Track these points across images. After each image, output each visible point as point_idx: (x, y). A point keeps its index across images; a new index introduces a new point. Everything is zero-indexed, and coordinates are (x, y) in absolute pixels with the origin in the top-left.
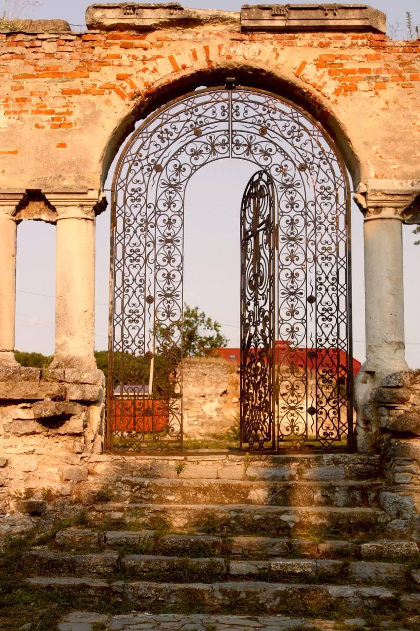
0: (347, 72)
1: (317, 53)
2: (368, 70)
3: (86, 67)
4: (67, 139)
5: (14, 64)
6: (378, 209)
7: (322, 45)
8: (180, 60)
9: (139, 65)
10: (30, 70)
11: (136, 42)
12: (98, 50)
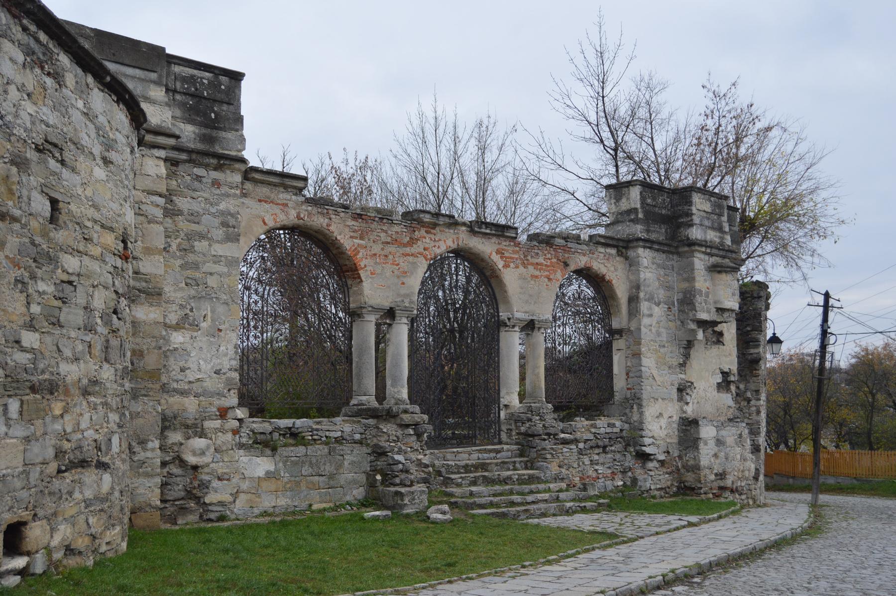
0: (506, 258)
1: (496, 247)
2: (512, 258)
3: (413, 241)
4: (405, 280)
5: (383, 235)
6: (514, 326)
7: (499, 244)
9: (432, 244)
10: (389, 239)
11: (432, 231)
12: (417, 233)
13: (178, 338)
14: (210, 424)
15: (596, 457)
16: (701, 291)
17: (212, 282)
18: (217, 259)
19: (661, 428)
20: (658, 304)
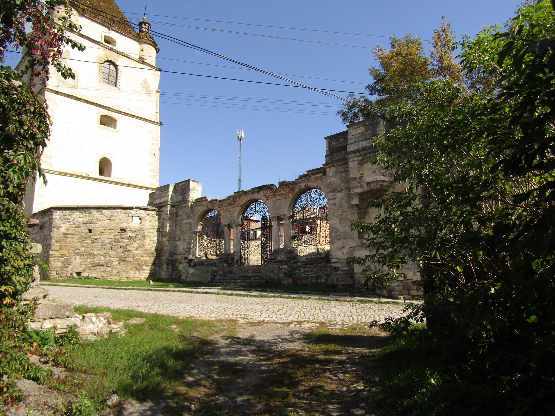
8: (246, 199)
13: (178, 243)
14: (183, 261)
15: (307, 269)
16: (354, 179)
17: (184, 229)
18: (185, 224)
19: (343, 253)
20: (340, 192)
